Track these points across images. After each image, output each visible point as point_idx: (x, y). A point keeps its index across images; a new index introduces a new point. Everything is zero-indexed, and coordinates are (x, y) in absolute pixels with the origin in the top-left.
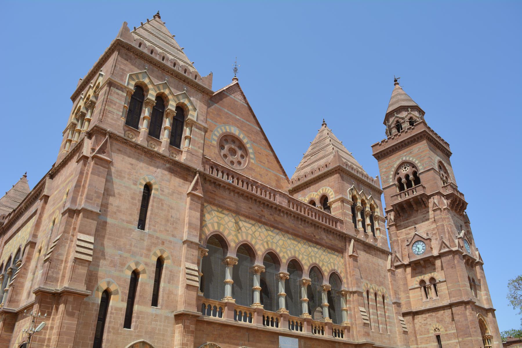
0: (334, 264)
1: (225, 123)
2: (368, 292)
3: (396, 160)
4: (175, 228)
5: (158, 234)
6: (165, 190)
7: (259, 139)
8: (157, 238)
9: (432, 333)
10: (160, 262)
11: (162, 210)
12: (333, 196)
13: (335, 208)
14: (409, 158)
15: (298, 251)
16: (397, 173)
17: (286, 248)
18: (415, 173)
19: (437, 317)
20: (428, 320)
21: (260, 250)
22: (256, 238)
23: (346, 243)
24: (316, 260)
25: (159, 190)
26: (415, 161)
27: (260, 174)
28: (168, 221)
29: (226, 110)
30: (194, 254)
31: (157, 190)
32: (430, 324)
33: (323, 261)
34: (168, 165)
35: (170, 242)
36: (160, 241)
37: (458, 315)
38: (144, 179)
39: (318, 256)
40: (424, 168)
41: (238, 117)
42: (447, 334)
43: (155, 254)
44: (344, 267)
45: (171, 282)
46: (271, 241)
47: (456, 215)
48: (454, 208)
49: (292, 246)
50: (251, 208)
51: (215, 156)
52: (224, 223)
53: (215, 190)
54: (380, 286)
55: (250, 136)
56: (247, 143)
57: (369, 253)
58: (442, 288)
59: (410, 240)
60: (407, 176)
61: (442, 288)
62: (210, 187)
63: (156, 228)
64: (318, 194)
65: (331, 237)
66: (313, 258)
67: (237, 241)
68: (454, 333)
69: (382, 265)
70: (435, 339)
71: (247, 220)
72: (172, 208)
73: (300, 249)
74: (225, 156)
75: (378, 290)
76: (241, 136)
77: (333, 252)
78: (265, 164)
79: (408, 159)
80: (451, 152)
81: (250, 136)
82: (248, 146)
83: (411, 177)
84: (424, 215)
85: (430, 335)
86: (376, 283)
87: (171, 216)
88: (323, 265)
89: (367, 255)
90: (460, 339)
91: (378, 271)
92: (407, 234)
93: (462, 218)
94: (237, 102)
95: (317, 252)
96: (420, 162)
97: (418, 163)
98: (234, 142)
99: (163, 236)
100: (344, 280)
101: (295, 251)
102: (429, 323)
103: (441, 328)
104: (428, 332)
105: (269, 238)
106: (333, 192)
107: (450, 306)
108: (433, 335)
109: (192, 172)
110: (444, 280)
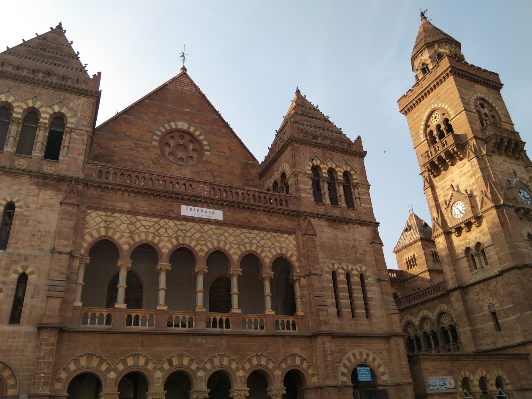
0: (281, 248)
1: (169, 121)
2: (334, 274)
3: (422, 112)
4: (43, 242)
5: (20, 251)
6: (31, 205)
7: (216, 127)
8: (19, 255)
9: (486, 310)
10: (23, 278)
11: (27, 226)
12: (289, 172)
13: (291, 184)
14: (438, 105)
15: (224, 241)
16: (427, 126)
17: (206, 240)
18: (446, 121)
19: (490, 291)
20: (480, 294)
21: (166, 247)
22: (160, 236)
23: (299, 221)
24: (251, 247)
25: (24, 207)
26: (445, 106)
27: (218, 165)
28: (34, 235)
29: (170, 106)
30: (63, 264)
31: (21, 207)
32: (483, 300)
33: (262, 247)
34: (36, 180)
35: (36, 256)
36: (23, 258)
37: (512, 284)
38: (5, 199)
39: (254, 241)
40: (455, 113)
41: (186, 110)
42: (503, 310)
43: (15, 272)
44: (295, 249)
45: (36, 296)
46: (183, 235)
47: (508, 160)
48: (503, 151)
49: (214, 237)
50: (153, 205)
51: (156, 156)
52: (114, 226)
53: (102, 194)
54: (356, 264)
55: (204, 127)
56: (200, 135)
57: (339, 228)
58: (492, 254)
59: (447, 203)
60: (438, 127)
61: (492, 253)
62: (95, 193)
63: (18, 245)
64: (279, 174)
65: (275, 219)
66: (247, 245)
67: (132, 243)
68: (511, 308)
69: (361, 239)
70: (490, 317)
71: (148, 218)
72: (40, 222)
73: (227, 238)
74: (171, 154)
75: (352, 269)
76: (192, 129)
77: (280, 235)
78: (225, 153)
79: (436, 106)
80: (502, 83)
81: (204, 127)
82: (202, 138)
83: (443, 127)
84: (461, 169)
85: (485, 313)
86: (348, 261)
87: (39, 231)
88: (263, 251)
89: (336, 232)
90: (519, 315)
91: (354, 247)
92: (445, 196)
93: (520, 162)
94: (185, 93)
95: (253, 238)
96: (449, 106)
97: (448, 108)
98: (182, 137)
99: (27, 252)
100: (296, 264)
101: (219, 242)
102: (481, 298)
103: (496, 303)
104: (482, 309)
105: (179, 233)
106: (288, 168)
107: (501, 273)
108: (488, 312)
109: (69, 181)
110: (491, 243)
